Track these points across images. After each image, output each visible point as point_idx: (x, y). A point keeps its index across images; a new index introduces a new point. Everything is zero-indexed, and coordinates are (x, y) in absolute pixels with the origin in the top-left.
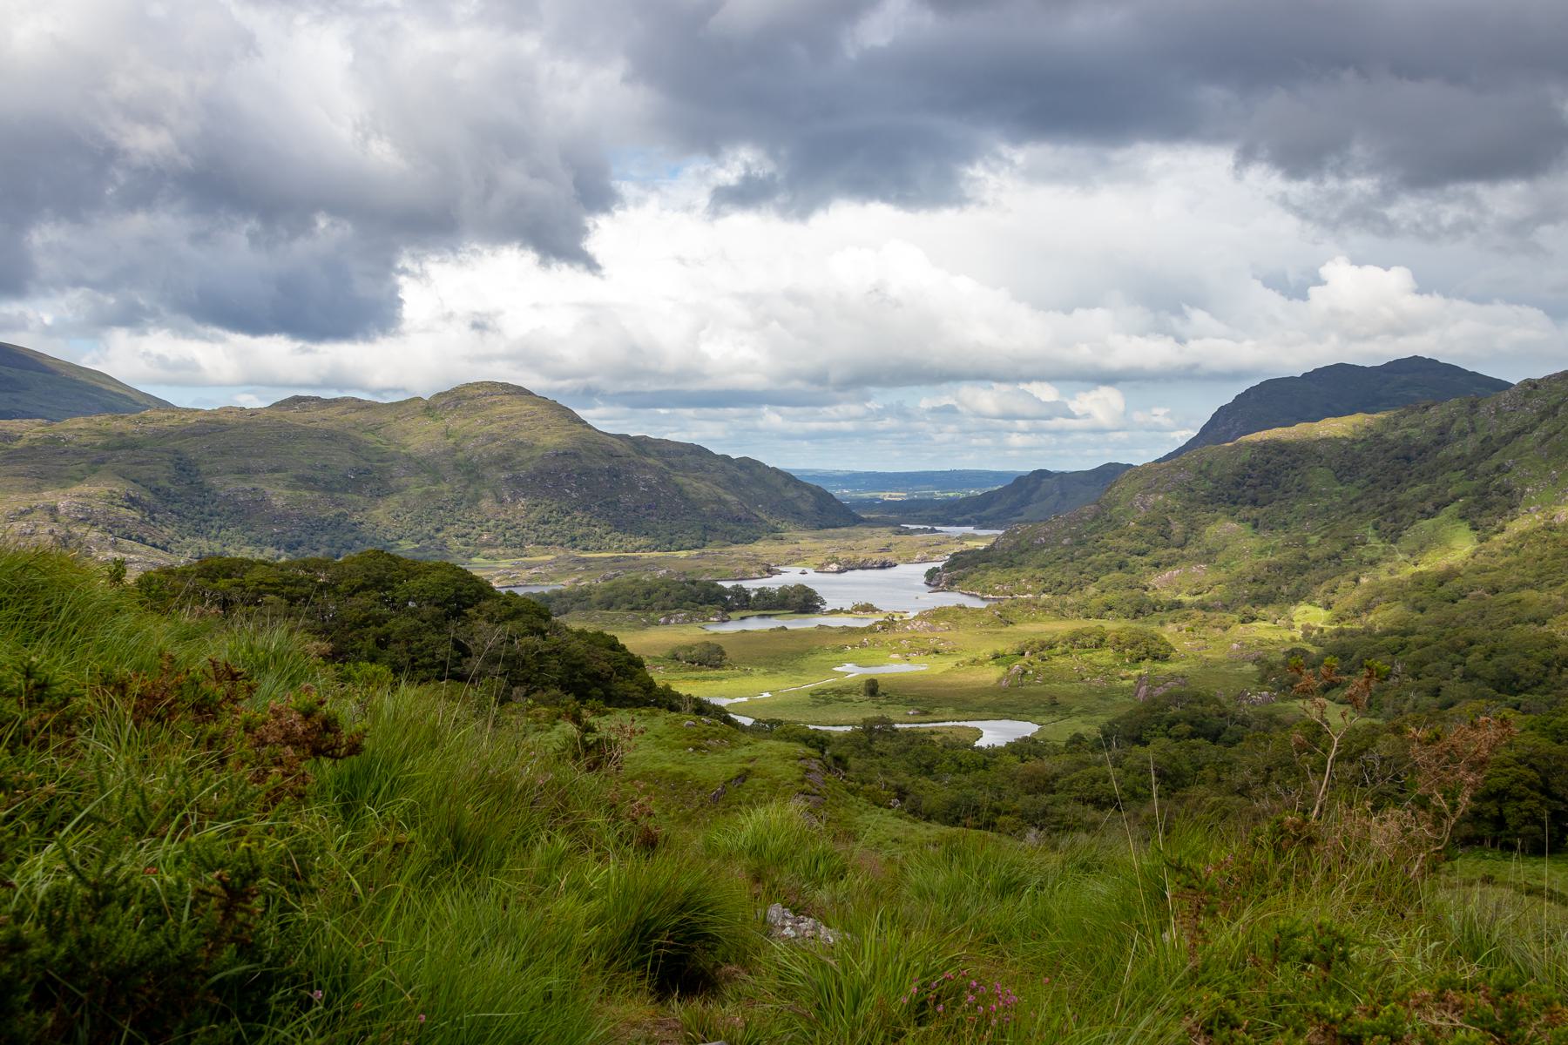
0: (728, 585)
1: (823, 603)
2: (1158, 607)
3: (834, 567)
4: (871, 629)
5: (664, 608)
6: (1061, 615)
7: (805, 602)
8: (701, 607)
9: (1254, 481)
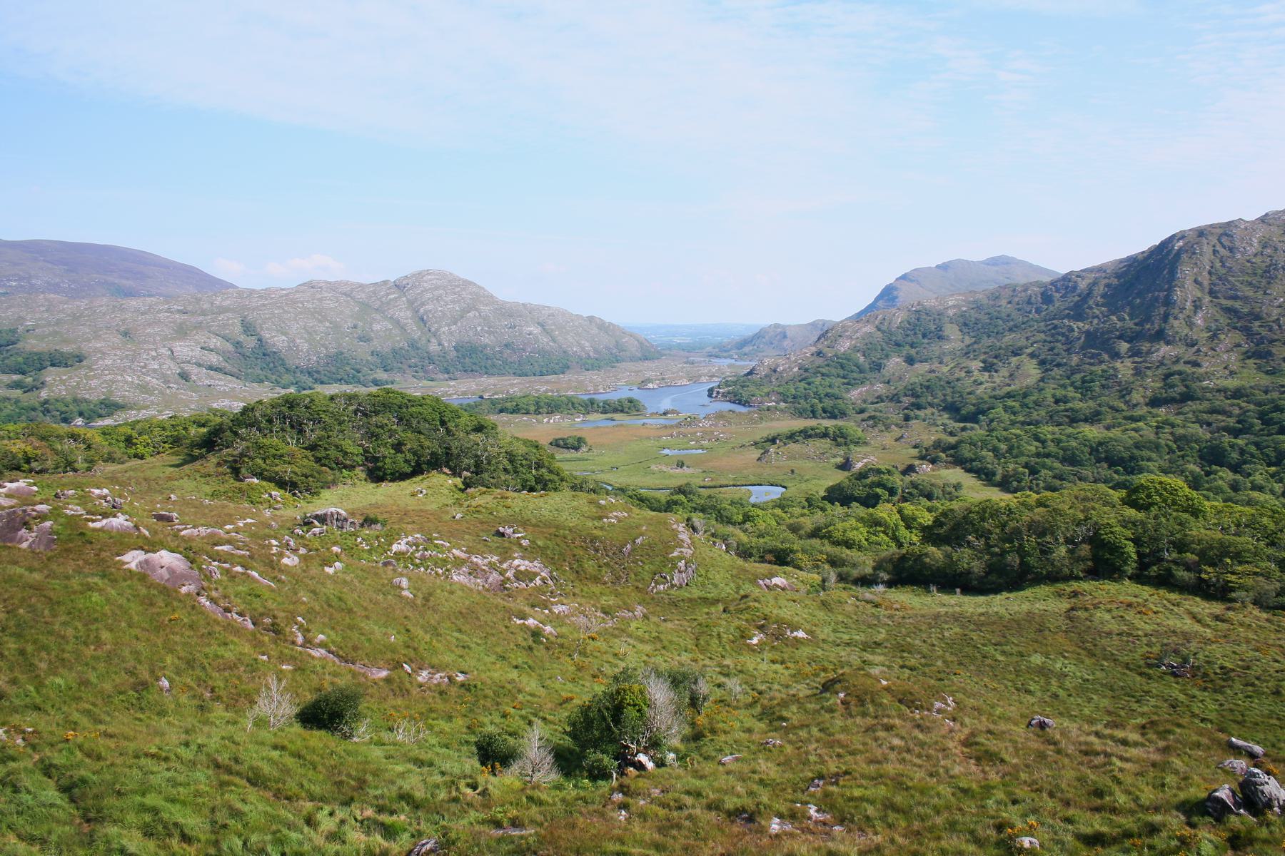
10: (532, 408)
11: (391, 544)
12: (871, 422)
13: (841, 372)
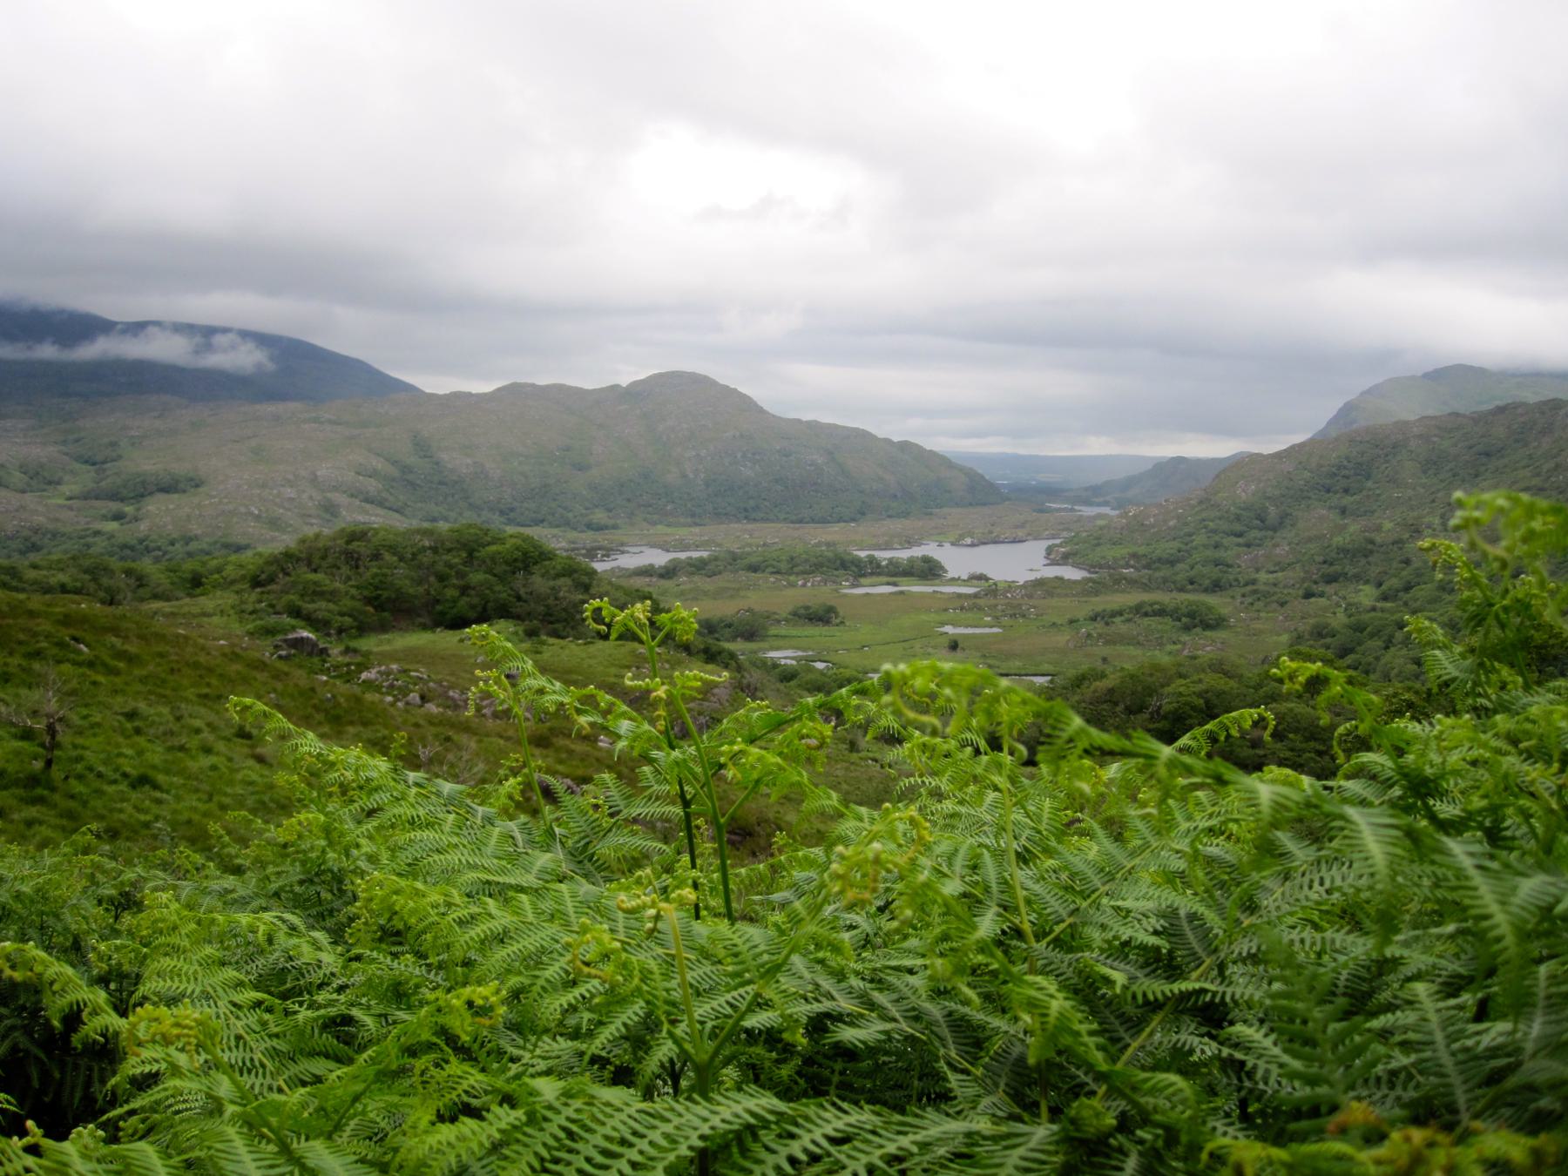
0: (863, 554)
1: (946, 571)
2: (1234, 583)
3: (969, 541)
4: (976, 596)
5: (804, 573)
6: (1146, 587)
7: (929, 570)
8: (836, 573)
9: (1347, 472)
10: (784, 566)
11: (361, 672)
12: (1250, 600)
13: (1238, 527)
